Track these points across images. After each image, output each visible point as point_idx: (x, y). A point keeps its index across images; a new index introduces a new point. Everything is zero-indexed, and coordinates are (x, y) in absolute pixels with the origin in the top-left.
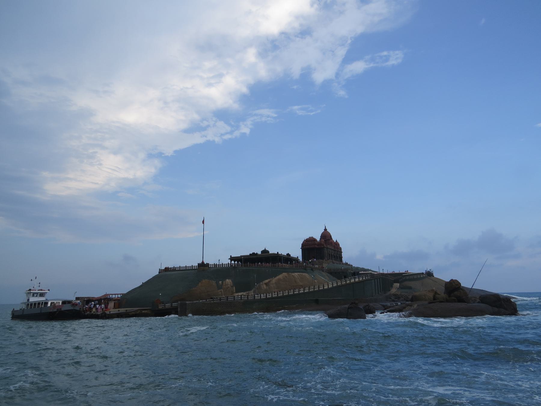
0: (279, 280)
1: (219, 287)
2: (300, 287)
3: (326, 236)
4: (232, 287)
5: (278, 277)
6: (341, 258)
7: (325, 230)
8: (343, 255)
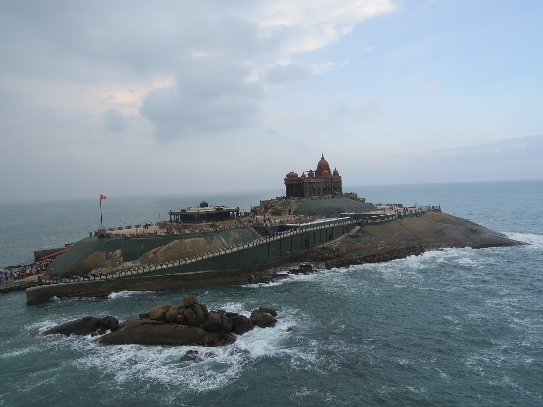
0: (169, 248)
1: (108, 258)
3: (323, 166)
4: (120, 257)
5: (168, 245)
7: (323, 158)
8: (343, 185)
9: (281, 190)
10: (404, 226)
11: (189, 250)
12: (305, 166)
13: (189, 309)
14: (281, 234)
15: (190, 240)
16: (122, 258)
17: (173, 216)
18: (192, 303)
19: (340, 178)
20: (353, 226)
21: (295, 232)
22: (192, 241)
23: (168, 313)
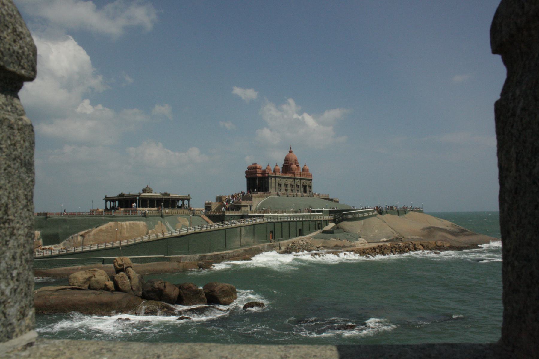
2: (125, 238)
4: (38, 239)
6: (310, 187)
9: (242, 186)
10: (385, 222)
11: (126, 235)
13: (122, 273)
15: (128, 223)
16: (41, 241)
17: (108, 203)
18: (125, 266)
19: (310, 175)
20: (326, 222)
21: (258, 221)
22: (130, 224)
23: (93, 278)
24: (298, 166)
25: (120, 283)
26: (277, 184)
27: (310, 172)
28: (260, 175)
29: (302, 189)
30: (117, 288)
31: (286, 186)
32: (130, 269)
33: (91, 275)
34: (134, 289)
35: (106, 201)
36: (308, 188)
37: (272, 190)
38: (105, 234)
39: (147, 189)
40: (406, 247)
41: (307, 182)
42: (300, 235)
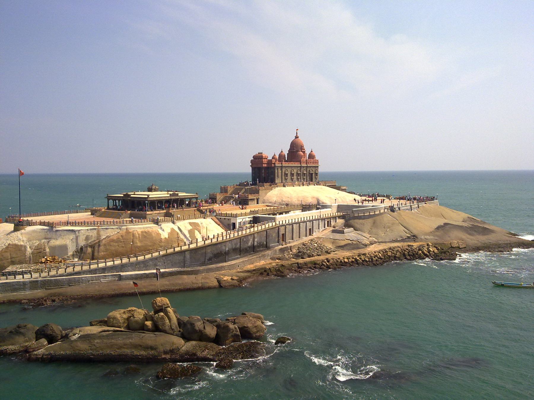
7: (297, 137)
8: (321, 170)
11: (139, 244)
12: (275, 147)
13: (162, 314)
14: (254, 227)
17: (111, 201)
19: (317, 162)
21: (271, 224)
24: (304, 152)
25: (160, 323)
26: (283, 174)
27: (317, 158)
28: (266, 165)
29: (308, 177)
30: (157, 328)
31: (292, 175)
32: (169, 309)
33: (129, 315)
34: (173, 328)
35: (108, 200)
36: (314, 175)
37: (278, 181)
38: (117, 244)
39: (153, 187)
40: (419, 250)
41: (314, 169)
42: (310, 235)
